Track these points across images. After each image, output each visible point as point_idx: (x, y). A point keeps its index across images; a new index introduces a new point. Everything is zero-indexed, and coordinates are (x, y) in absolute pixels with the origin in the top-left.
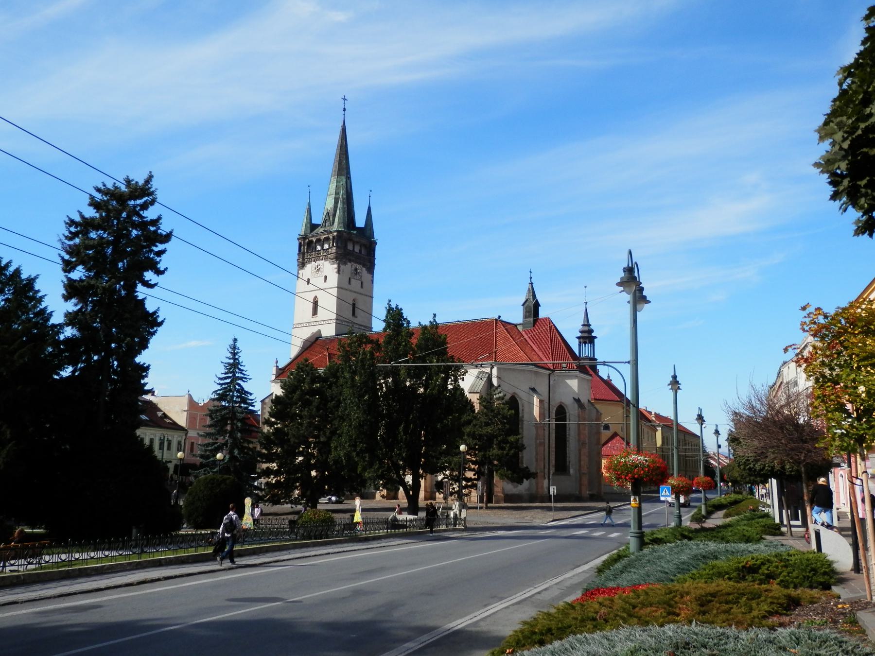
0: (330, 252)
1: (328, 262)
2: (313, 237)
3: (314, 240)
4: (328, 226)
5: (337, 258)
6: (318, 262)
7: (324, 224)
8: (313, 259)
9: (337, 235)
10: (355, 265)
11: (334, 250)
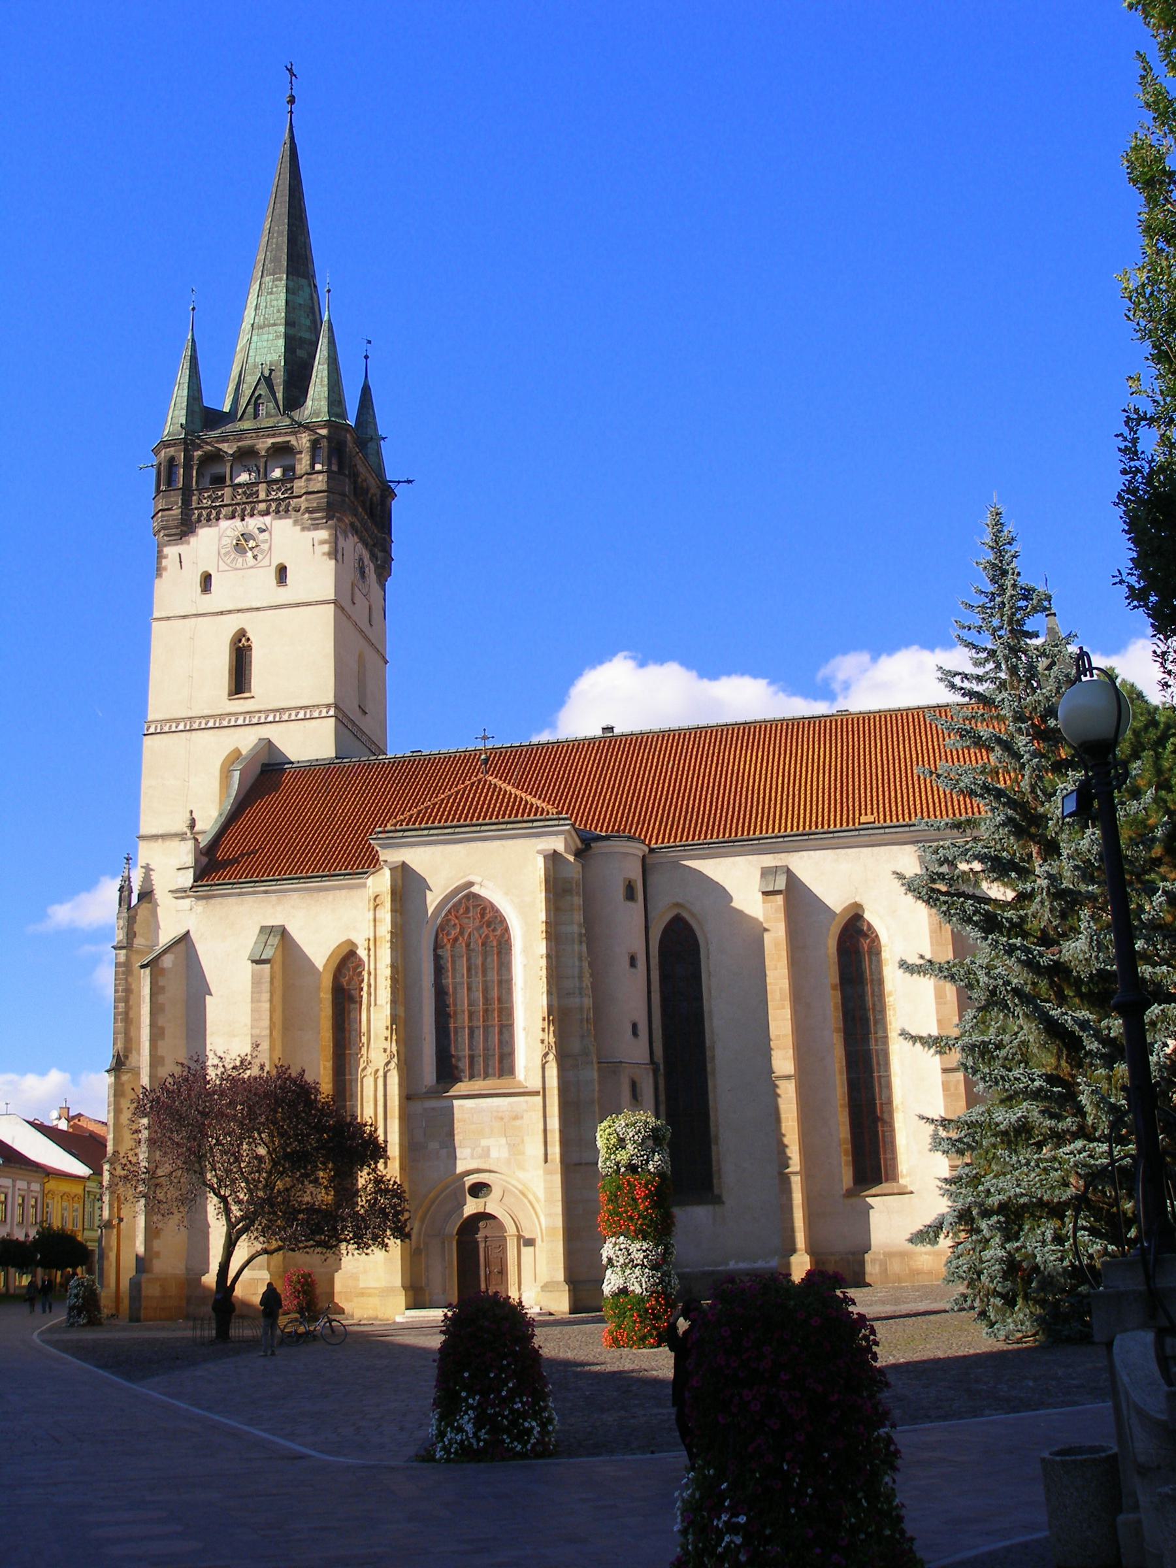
1: (289, 522)
2: (224, 439)
3: (229, 448)
4: (268, 415)
6: (253, 523)
8: (224, 511)
9: (329, 438)
10: (360, 545)
11: (320, 482)
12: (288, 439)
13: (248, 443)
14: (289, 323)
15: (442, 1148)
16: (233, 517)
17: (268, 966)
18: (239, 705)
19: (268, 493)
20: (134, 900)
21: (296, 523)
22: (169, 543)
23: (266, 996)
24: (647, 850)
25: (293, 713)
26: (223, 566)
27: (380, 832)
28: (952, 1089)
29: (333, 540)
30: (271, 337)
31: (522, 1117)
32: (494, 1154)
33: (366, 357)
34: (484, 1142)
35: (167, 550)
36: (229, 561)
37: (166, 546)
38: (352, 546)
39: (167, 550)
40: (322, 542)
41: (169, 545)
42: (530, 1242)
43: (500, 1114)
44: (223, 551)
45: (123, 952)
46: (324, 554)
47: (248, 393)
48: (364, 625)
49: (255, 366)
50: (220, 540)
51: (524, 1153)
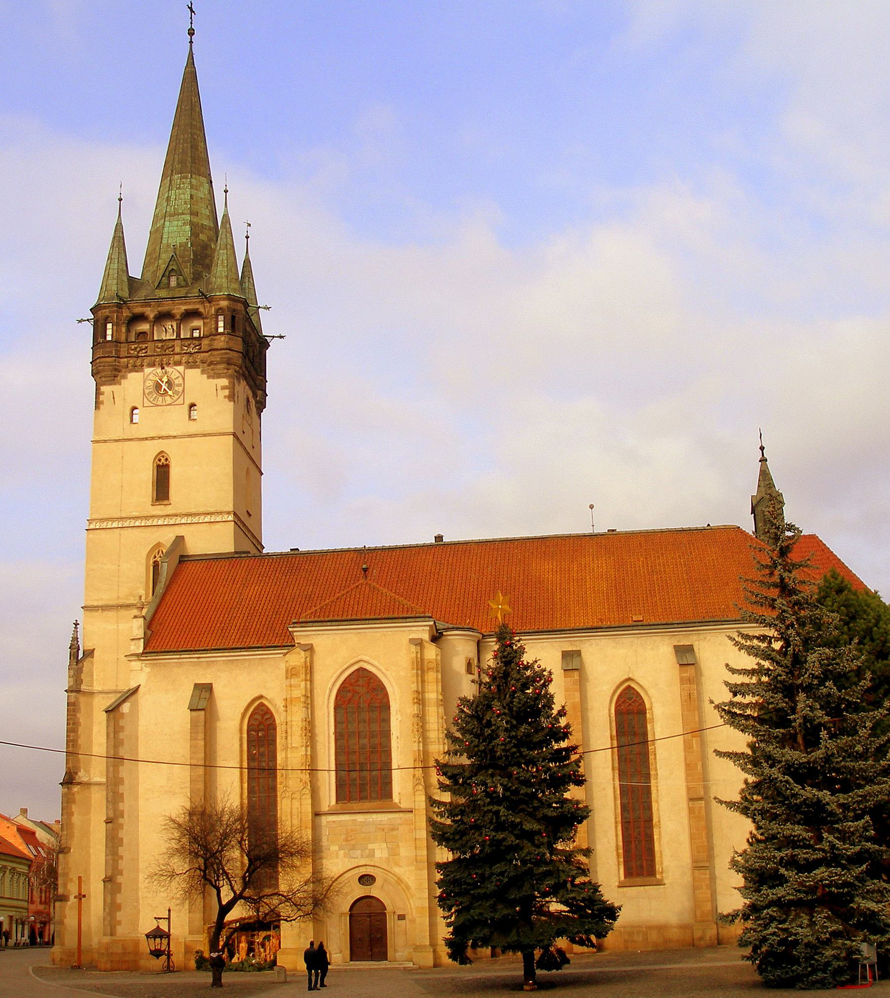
1: (198, 371)
2: (147, 305)
3: (151, 313)
4: (179, 285)
5: (229, 363)
7: (165, 280)
8: (147, 360)
12: (197, 307)
13: (164, 308)
14: (194, 213)
15: (340, 850)
16: (154, 365)
17: (202, 713)
18: (159, 510)
19: (182, 349)
20: (81, 655)
21: (203, 372)
22: (104, 384)
23: (201, 736)
24: (481, 636)
25: (202, 517)
26: (147, 403)
27: (296, 623)
28: (697, 812)
29: (231, 386)
30: (180, 223)
31: (398, 829)
32: (378, 854)
33: (247, 237)
34: (370, 846)
35: (103, 388)
36: (151, 399)
37: (103, 385)
38: (243, 389)
39: (103, 388)
40: (223, 388)
41: (105, 385)
42: (402, 917)
43: (382, 827)
44: (147, 391)
45: (73, 694)
46: (225, 397)
47: (163, 267)
48: (249, 449)
49: (168, 246)
50: (144, 383)
51: (399, 854)
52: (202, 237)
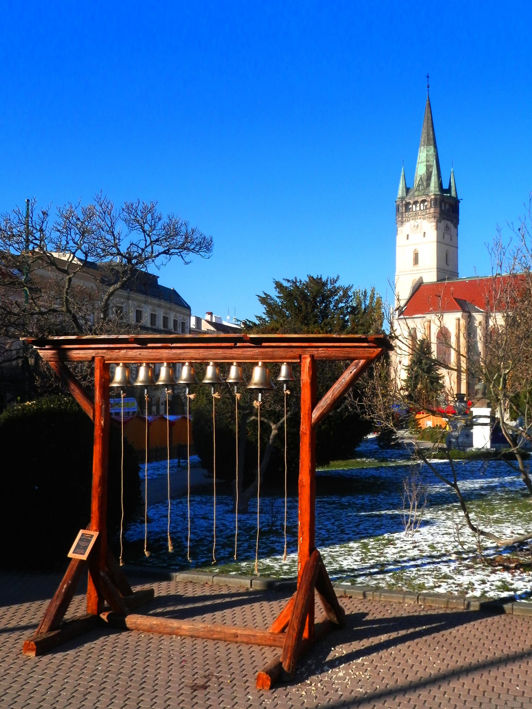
0: (428, 213)
1: (425, 221)
2: (410, 199)
4: (422, 190)
5: (435, 217)
11: (432, 210)
13: (416, 199)
14: (427, 161)
18: (416, 268)
52: (430, 169)
